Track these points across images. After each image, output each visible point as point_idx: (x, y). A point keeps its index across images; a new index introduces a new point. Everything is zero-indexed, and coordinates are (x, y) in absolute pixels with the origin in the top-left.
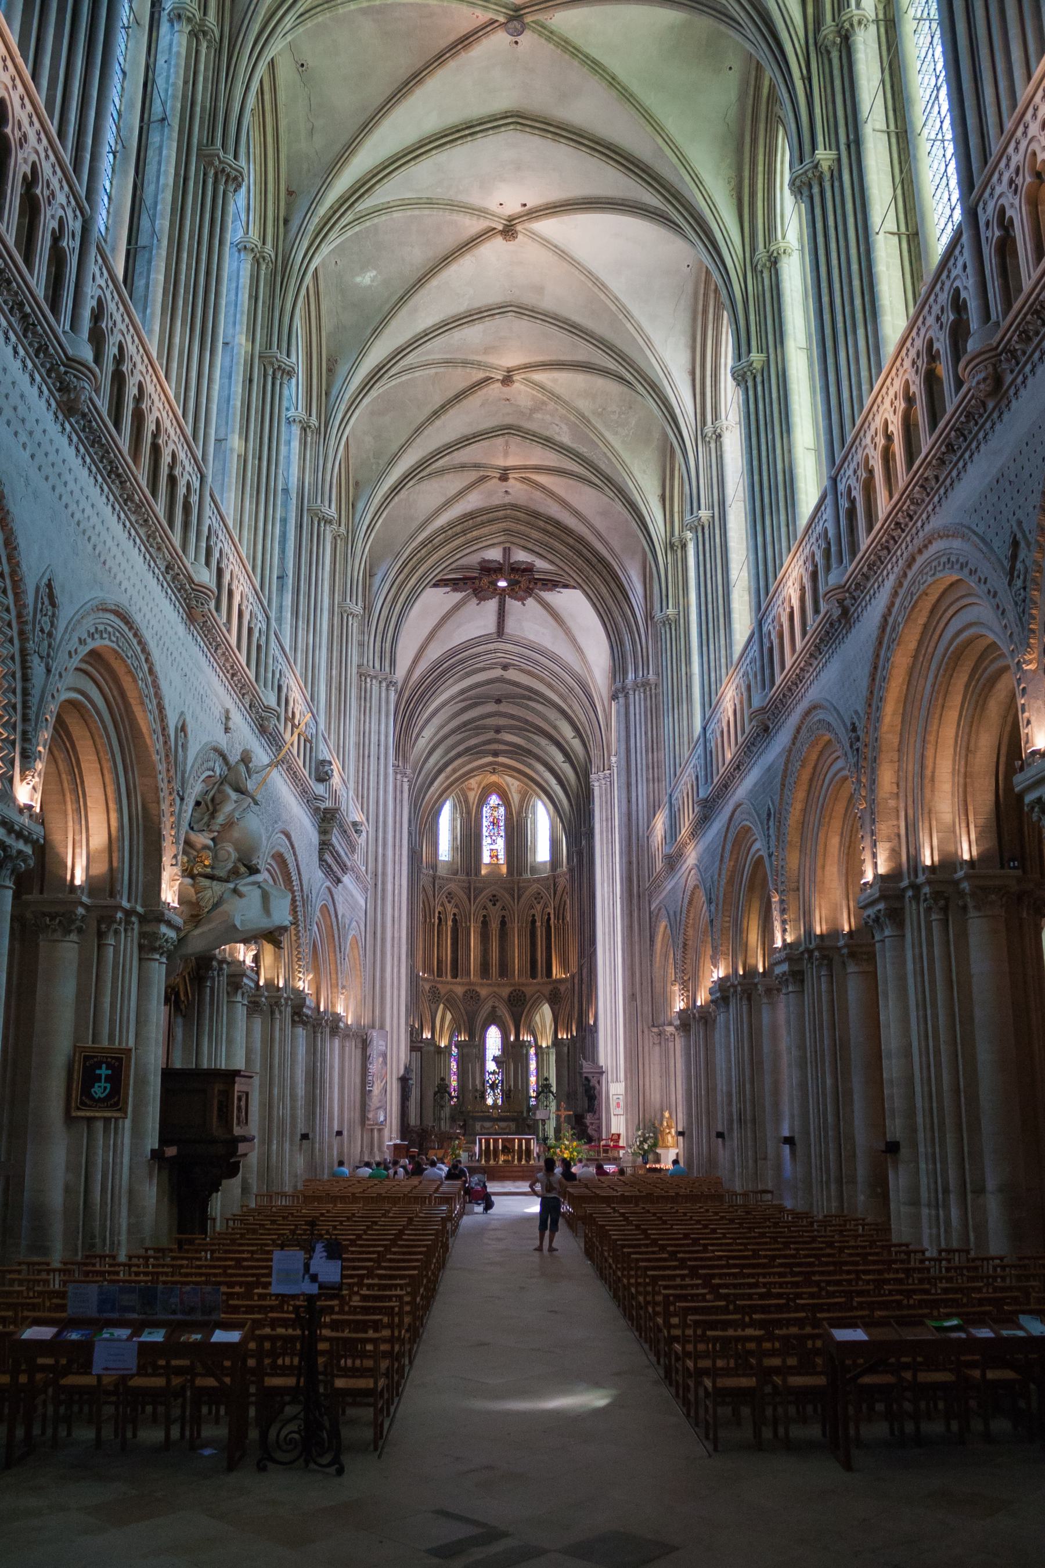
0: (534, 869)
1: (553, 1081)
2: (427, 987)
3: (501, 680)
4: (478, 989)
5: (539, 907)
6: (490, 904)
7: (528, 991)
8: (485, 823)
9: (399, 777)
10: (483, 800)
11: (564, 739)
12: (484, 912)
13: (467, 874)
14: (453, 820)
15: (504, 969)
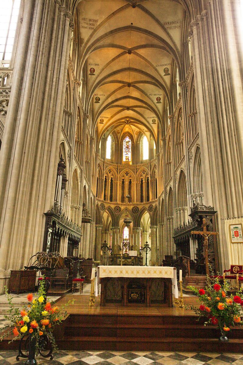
0: (142, 163)
1: (149, 243)
2: (100, 203)
3: (131, 28)
4: (120, 206)
5: (144, 175)
6: (125, 175)
7: (140, 207)
8: (124, 147)
9: (62, 14)
10: (123, 138)
11: (160, 75)
12: (123, 178)
13: (117, 163)
14: (112, 145)
15: (130, 199)
